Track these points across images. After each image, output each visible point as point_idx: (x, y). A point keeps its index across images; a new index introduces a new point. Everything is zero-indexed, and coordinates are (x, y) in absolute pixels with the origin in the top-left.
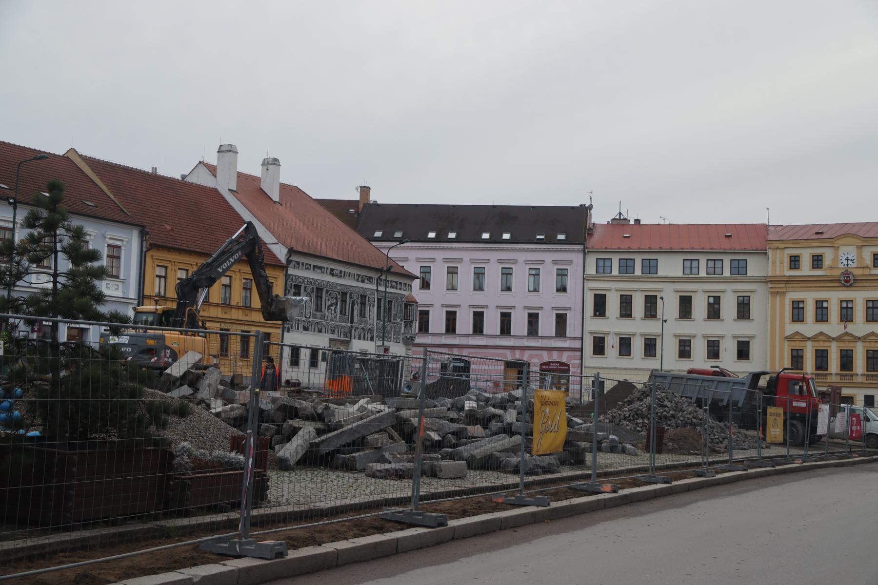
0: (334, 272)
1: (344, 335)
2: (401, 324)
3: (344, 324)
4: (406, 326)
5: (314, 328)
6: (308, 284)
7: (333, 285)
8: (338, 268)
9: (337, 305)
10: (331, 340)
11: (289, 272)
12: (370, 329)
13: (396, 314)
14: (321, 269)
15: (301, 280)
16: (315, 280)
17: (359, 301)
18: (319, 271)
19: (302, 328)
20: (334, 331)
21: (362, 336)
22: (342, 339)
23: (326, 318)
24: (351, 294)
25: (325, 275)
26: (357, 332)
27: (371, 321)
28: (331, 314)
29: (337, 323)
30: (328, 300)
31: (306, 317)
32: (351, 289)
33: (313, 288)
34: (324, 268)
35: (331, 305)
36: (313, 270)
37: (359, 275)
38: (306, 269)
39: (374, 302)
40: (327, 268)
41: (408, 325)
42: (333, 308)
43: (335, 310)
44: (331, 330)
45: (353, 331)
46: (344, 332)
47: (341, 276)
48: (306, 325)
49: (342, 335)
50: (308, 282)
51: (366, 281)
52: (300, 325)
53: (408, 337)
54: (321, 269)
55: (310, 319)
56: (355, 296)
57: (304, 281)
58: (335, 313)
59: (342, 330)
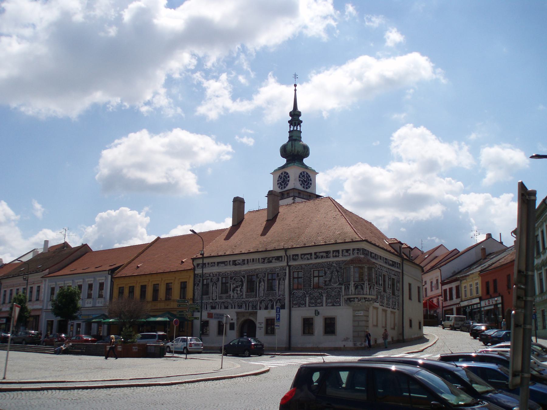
0: (237, 262)
2: (341, 288)
3: (251, 299)
5: (221, 306)
6: (214, 276)
7: (236, 273)
9: (242, 285)
10: (238, 314)
11: (196, 272)
13: (330, 281)
14: (225, 263)
15: (208, 275)
16: (219, 273)
17: (266, 279)
18: (223, 265)
19: (210, 308)
20: (241, 306)
21: (270, 306)
22: (249, 311)
23: (231, 298)
24: (257, 275)
27: (281, 293)
28: (237, 294)
29: (243, 300)
30: (233, 284)
31: (213, 300)
33: (218, 278)
34: (227, 262)
35: (237, 287)
36: (218, 265)
37: (264, 259)
38: (211, 266)
39: (285, 275)
40: (230, 261)
41: (346, 288)
42: (239, 289)
43: (241, 290)
44: (238, 306)
45: (259, 303)
46: (253, 305)
47: (244, 264)
48: (214, 305)
49: (250, 308)
50: (213, 275)
51: (274, 261)
52: (208, 306)
53: (346, 299)
54: (225, 263)
55: (216, 301)
56: (261, 276)
57: (210, 275)
59: (250, 304)
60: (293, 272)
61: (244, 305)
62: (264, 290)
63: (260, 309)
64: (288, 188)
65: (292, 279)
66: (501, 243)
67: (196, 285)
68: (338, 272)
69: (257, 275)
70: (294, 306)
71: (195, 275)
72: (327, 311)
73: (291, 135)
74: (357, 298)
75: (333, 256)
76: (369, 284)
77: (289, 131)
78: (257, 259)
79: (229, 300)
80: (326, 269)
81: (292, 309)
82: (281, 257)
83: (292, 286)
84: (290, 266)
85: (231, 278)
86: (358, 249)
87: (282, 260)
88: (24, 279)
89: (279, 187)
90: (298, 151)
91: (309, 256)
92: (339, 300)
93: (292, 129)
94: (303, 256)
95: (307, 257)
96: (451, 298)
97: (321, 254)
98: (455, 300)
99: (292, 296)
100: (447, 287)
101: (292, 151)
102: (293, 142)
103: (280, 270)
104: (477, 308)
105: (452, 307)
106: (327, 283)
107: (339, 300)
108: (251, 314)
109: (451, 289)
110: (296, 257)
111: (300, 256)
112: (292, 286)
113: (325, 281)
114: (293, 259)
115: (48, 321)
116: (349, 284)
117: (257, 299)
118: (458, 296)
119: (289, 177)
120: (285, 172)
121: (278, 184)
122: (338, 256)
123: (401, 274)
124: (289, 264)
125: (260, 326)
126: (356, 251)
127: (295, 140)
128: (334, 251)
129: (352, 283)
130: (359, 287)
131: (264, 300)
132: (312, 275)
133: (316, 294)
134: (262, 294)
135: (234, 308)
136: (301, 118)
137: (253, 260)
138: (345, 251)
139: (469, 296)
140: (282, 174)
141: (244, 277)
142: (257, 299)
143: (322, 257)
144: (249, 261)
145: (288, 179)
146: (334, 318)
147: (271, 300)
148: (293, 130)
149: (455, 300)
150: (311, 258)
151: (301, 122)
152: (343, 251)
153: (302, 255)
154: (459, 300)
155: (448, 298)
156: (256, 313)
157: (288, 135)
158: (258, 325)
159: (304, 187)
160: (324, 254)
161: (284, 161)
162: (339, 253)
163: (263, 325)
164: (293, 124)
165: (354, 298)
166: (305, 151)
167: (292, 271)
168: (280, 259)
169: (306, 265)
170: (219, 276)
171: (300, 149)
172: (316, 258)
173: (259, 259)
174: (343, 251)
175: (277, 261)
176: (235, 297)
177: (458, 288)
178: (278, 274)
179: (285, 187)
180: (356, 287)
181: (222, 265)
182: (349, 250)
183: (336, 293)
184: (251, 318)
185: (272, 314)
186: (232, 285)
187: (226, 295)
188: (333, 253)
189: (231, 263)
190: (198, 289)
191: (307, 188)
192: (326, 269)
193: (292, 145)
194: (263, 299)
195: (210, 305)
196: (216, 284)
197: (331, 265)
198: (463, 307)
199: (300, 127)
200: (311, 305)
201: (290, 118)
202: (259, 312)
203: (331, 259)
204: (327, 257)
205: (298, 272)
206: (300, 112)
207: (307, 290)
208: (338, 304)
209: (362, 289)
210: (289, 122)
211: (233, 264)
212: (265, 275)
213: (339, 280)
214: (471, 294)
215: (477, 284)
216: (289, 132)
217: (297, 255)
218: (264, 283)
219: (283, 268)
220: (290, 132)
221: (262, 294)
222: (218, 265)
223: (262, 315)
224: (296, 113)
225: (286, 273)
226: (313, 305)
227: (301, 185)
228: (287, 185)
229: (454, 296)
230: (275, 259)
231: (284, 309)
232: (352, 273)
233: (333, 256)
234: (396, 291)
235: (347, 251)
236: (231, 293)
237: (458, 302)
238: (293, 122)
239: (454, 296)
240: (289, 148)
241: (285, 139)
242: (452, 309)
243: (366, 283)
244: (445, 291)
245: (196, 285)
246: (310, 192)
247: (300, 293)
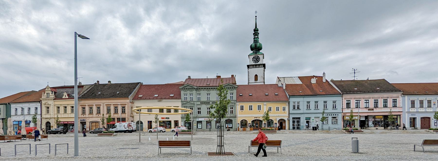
64: (258, 63)
119: (259, 58)
120: (257, 56)
140: (255, 56)
145: (259, 59)
179: (257, 63)
228: (259, 62)
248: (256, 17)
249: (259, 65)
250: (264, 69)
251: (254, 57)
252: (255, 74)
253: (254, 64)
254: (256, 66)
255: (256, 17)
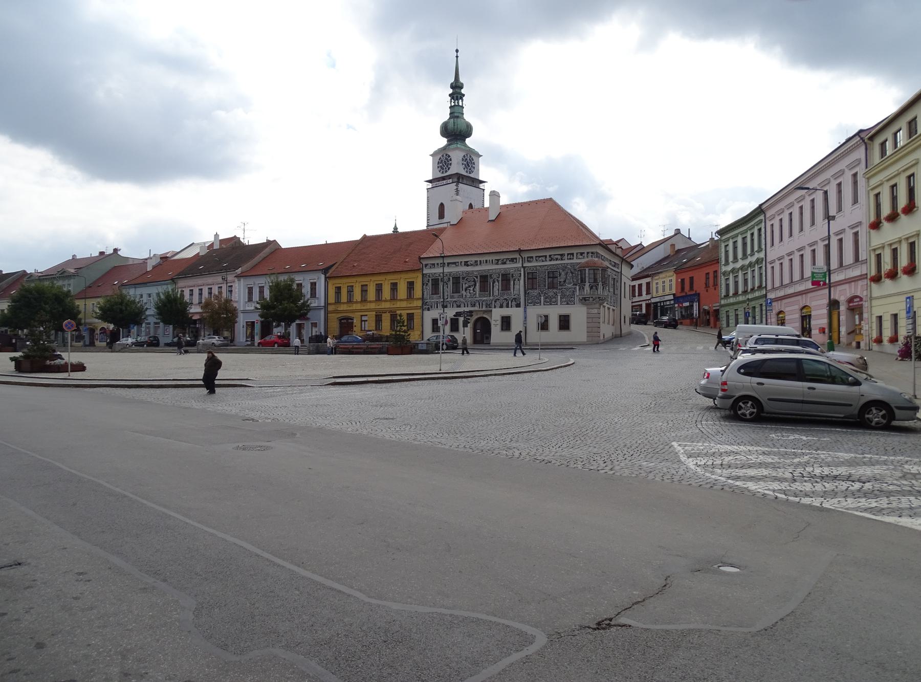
0: (469, 263)
1: (486, 307)
2: (575, 288)
4: (580, 289)
5: (453, 305)
7: (468, 273)
8: (474, 259)
9: (475, 285)
12: (515, 299)
13: (565, 281)
14: (456, 264)
15: (438, 275)
17: (500, 279)
19: (441, 307)
20: (475, 305)
21: (505, 304)
22: (483, 309)
23: (464, 297)
24: (491, 275)
25: (459, 267)
26: (497, 302)
28: (470, 293)
29: (476, 299)
30: (465, 284)
32: (491, 271)
33: (449, 278)
34: (458, 262)
36: (448, 266)
37: (498, 260)
39: (520, 276)
40: (461, 262)
42: (472, 289)
43: (473, 290)
44: (471, 304)
46: (486, 304)
47: (477, 265)
49: (484, 307)
53: (581, 298)
54: (456, 264)
56: (495, 276)
57: (439, 276)
58: (474, 291)
59: (484, 303)
60: (528, 273)
61: (477, 304)
62: (498, 290)
63: (495, 307)
64: (448, 173)
65: (527, 280)
66: (690, 238)
67: (425, 284)
68: (572, 273)
69: (491, 275)
70: (529, 305)
71: (423, 274)
72: (564, 310)
73: (452, 112)
74: (592, 297)
75: (568, 259)
76: (602, 285)
77: (450, 106)
78: (491, 261)
79: (461, 299)
80: (561, 271)
81: (527, 307)
82: (516, 259)
83: (527, 286)
84: (524, 268)
85: (463, 278)
86: (592, 253)
87: (516, 262)
88: (223, 279)
89: (440, 171)
90: (460, 130)
91: (544, 259)
92: (573, 299)
93: (453, 104)
94: (537, 258)
95: (542, 259)
96: (640, 294)
97: (556, 257)
98: (644, 296)
99: (527, 295)
100: (636, 283)
101: (454, 130)
102: (455, 119)
103: (515, 271)
104: (670, 304)
105: (640, 303)
106: (562, 283)
107: (573, 299)
108: (485, 312)
109: (640, 286)
110: (531, 259)
111: (534, 259)
112: (527, 286)
113: (560, 282)
114: (528, 261)
115: (247, 322)
116: (585, 285)
117: (491, 298)
118: (648, 293)
119: (451, 160)
120: (446, 155)
121: (438, 167)
122: (573, 259)
123: (620, 274)
124: (524, 265)
125: (496, 323)
126: (590, 255)
127: (458, 117)
128: (568, 254)
129: (587, 284)
130: (594, 287)
131: (499, 299)
132: (547, 276)
133: (551, 294)
134: (496, 293)
135: (467, 307)
136: (463, 91)
137: (486, 261)
138: (579, 254)
139: (661, 293)
140: (443, 156)
141: (477, 277)
142: (491, 298)
143: (557, 259)
144: (482, 262)
145: (450, 162)
146: (569, 315)
147: (505, 299)
148: (455, 105)
149: (644, 296)
150: (546, 260)
151: (464, 95)
152: (577, 254)
153: (536, 257)
154: (649, 297)
155: (637, 294)
156: (491, 311)
157: (448, 111)
158: (493, 323)
159: (467, 172)
160: (559, 257)
161: (443, 142)
162: (573, 256)
163: (499, 322)
164: (455, 98)
165: (589, 297)
166: (467, 132)
167: (526, 272)
168: (515, 261)
169: (540, 266)
170: (450, 275)
171: (463, 127)
172: (550, 261)
173: (492, 260)
174: (577, 254)
175: (511, 262)
176: (468, 296)
177: (648, 284)
178: (512, 274)
179: (446, 172)
180: (591, 288)
181: (453, 265)
182: (584, 253)
183: (571, 293)
184: (485, 316)
185: (506, 312)
186: (464, 285)
187: (458, 294)
188: (568, 256)
189: (463, 263)
190: (427, 289)
191: (470, 173)
192: (561, 271)
193: (454, 123)
194: (497, 298)
195: (441, 305)
196: (447, 284)
197: (566, 267)
198: (654, 303)
199: (462, 101)
200: (546, 304)
201: (451, 91)
202: (494, 310)
203: (566, 261)
204: (562, 260)
205: (532, 273)
206: (462, 84)
207: (542, 290)
208: (573, 303)
209: (597, 289)
210: (450, 95)
211: (465, 265)
212: (499, 276)
213: (573, 281)
214: (664, 290)
215: (671, 281)
216: (450, 108)
217: (532, 257)
218: (498, 282)
219: (518, 269)
220: (451, 107)
221: (496, 293)
222: (448, 266)
223: (497, 314)
224: (458, 84)
225: (520, 274)
226: (548, 304)
227: (464, 169)
229: (644, 292)
230: (510, 261)
231: (520, 307)
232: (587, 275)
233: (568, 259)
234: (616, 290)
235: (582, 254)
236: (464, 292)
237: (648, 298)
238: (455, 96)
239: (644, 292)
240: (451, 126)
241: (445, 116)
242: (641, 305)
243: (600, 284)
244: (634, 287)
245: (425, 284)
246: (473, 177)
247: (535, 293)
248: (457, 51)
249: (450, 177)
250: (455, 187)
251: (440, 158)
252: (440, 203)
253: (440, 175)
254: (443, 178)
255: (457, 51)
